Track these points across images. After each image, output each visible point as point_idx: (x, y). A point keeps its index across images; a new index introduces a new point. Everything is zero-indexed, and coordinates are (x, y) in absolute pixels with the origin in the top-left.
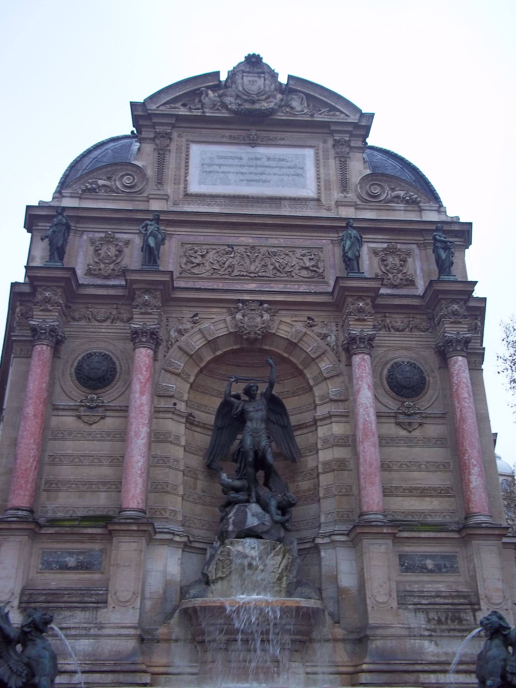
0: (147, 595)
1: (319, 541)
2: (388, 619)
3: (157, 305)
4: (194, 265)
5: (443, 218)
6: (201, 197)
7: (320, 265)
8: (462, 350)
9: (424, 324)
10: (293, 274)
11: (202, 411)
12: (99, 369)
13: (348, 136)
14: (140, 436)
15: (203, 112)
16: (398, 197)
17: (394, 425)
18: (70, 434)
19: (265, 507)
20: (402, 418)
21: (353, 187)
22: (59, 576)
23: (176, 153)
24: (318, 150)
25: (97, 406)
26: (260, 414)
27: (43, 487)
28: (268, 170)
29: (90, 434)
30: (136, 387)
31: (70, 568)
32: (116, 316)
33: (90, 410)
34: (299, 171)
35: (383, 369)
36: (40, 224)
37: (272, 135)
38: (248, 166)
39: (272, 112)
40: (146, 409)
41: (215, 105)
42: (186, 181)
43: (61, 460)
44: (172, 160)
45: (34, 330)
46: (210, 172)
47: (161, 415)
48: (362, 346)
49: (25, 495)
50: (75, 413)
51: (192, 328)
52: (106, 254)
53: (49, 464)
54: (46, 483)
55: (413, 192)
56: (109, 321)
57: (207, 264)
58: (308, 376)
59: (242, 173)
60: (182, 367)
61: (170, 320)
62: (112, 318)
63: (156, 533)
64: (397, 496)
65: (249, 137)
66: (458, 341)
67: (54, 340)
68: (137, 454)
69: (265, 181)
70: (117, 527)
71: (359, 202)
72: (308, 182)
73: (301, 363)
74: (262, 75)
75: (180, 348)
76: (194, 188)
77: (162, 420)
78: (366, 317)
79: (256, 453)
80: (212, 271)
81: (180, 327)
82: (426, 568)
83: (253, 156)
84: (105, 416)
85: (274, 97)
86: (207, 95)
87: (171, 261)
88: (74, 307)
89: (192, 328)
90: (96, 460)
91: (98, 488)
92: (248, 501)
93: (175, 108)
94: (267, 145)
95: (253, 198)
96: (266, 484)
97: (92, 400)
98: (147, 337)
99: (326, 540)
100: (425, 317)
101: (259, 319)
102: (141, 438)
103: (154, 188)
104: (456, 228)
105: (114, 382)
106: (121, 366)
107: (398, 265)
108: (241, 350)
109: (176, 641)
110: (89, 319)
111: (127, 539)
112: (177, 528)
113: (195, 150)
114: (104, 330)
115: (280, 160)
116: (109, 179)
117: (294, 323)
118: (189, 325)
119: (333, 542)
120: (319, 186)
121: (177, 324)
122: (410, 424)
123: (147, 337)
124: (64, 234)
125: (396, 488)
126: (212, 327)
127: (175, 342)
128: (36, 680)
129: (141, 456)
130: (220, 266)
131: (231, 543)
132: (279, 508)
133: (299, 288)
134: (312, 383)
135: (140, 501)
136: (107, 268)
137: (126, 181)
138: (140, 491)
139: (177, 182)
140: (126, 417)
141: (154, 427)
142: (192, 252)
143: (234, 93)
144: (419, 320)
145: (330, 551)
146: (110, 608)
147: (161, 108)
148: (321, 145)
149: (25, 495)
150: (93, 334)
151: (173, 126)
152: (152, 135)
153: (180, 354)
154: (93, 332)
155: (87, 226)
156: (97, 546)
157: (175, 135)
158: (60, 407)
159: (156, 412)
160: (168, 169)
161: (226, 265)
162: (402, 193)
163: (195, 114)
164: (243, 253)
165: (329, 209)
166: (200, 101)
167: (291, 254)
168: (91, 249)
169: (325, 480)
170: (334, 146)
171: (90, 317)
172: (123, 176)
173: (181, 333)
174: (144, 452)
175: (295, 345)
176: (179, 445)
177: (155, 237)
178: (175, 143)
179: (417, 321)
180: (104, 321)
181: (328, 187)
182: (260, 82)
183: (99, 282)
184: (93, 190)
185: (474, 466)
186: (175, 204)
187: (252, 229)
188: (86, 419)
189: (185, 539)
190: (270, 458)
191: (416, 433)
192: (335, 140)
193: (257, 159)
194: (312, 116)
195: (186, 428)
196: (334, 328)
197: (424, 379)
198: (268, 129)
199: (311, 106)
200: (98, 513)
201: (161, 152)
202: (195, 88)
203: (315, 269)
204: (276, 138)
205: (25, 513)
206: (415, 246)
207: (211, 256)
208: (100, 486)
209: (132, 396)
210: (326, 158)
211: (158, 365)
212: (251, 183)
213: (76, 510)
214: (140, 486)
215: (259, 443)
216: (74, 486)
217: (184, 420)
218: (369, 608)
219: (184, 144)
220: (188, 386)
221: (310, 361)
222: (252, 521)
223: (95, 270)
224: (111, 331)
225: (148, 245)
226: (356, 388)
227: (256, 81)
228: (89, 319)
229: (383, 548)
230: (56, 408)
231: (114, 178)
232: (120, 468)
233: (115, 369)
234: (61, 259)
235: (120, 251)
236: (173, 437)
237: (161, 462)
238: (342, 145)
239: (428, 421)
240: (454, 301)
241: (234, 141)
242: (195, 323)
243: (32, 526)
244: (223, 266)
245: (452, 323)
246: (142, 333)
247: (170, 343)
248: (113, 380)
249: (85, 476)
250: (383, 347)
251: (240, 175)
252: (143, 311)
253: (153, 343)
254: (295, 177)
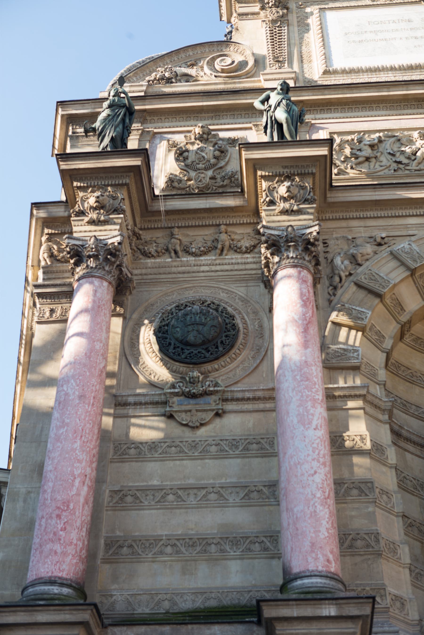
3: (309, 197)
4: (360, 159)
11: (413, 415)
12: (204, 325)
14: (310, 423)
23: (299, 26)
25: (206, 394)
27: (101, 554)
29: (194, 446)
32: (227, 244)
33: (192, 401)
43: (137, 498)
49: (64, 554)
50: (161, 410)
51: (375, 253)
52: (198, 156)
53: (114, 509)
54: (108, 545)
57: (382, 158)
59: (416, 38)
60: (369, 316)
61: (331, 243)
62: (220, 246)
68: (310, 459)
75: (359, 286)
84: (224, 412)
89: (375, 253)
90: (213, 496)
91: (222, 551)
98: (298, 249)
102: (314, 426)
105: (235, 350)
106: (245, 323)
110: (176, 252)
118: (369, 249)
121: (346, 247)
123: (298, 249)
124: (123, 120)
127: (346, 276)
129: (318, 461)
130: (409, 158)
135: (331, 557)
136: (203, 175)
138: (326, 534)
149: (64, 554)
150: (186, 275)
153: (362, 294)
154: (184, 273)
158: (131, 400)
171: (178, 248)
174: (324, 456)
176: (384, 463)
178: (295, 15)
180: (204, 253)
188: (184, 418)
205: (65, 591)
208: (228, 548)
213: (177, 599)
214: (324, 523)
216: (169, 550)
217: (386, 417)
224: (218, 268)
228: (176, 252)
232: (266, 508)
237: (355, 492)
242: (380, 245)
244: (413, 158)
246: (287, 241)
247: (337, 279)
248: (232, 346)
249: (192, 529)
253: (310, 261)
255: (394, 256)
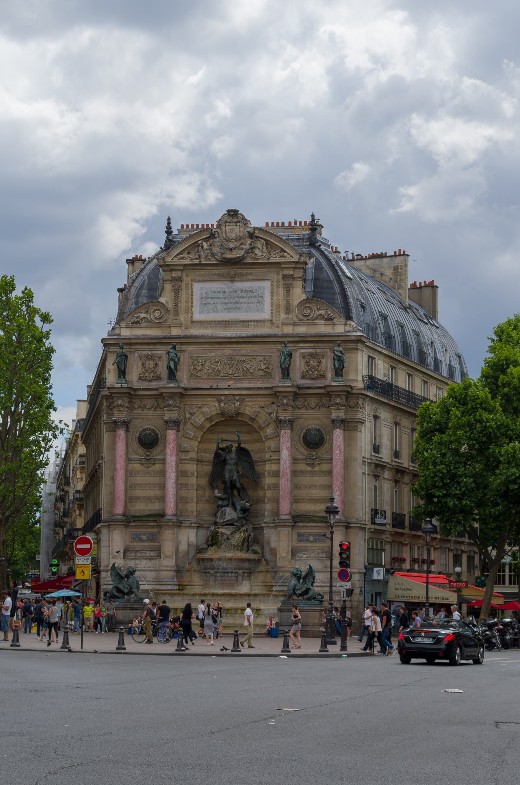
0: (180, 551)
1: (263, 525)
2: (286, 564)
5: (348, 328)
6: (201, 323)
7: (270, 367)
8: (340, 425)
9: (328, 403)
10: (254, 374)
13: (292, 270)
15: (200, 261)
16: (321, 315)
17: (304, 465)
18: (138, 473)
19: (235, 509)
20: (309, 461)
21: (294, 308)
22: (140, 544)
24: (272, 282)
25: (151, 459)
26: (234, 461)
27: (128, 501)
28: (242, 300)
29: (148, 473)
30: (168, 452)
31: (144, 541)
34: (260, 299)
35: (301, 432)
36: (110, 348)
37: (244, 271)
38: (229, 298)
39: (243, 258)
40: (174, 464)
41: (207, 256)
42: (192, 311)
44: (183, 295)
45: (115, 422)
46: (206, 304)
47: (183, 462)
48: (285, 425)
50: (140, 462)
51: (198, 411)
54: (129, 499)
55: (331, 311)
56: (153, 409)
57: (205, 370)
58: (262, 435)
61: (186, 406)
63: (182, 523)
64: (303, 503)
65: (229, 275)
66: (337, 421)
67: (126, 426)
69: (239, 309)
70: (162, 524)
71: (296, 319)
72: (265, 307)
73: (259, 427)
74: (238, 224)
75: (192, 424)
76: (197, 316)
77: (184, 465)
78: (288, 408)
79: (231, 482)
80: (208, 374)
81: (191, 411)
82: (310, 540)
83: (232, 290)
85: (245, 245)
86: (202, 247)
87: (185, 368)
88: (134, 400)
89: (198, 411)
92: (227, 506)
93: (182, 258)
94: (241, 280)
95: (231, 321)
96: (239, 495)
97: (147, 455)
99: (266, 525)
100: (328, 399)
101: (233, 406)
103: (173, 318)
104: (353, 338)
107: (316, 365)
108: (226, 420)
109: (195, 571)
111: (168, 528)
112: (193, 519)
113: (197, 286)
114: (151, 414)
115: (249, 291)
116: (147, 312)
117: (254, 406)
118: (196, 410)
119: (268, 526)
120: (272, 310)
122: (313, 464)
125: (303, 499)
126: (208, 411)
128: (133, 590)
131: (218, 528)
132: (241, 510)
133: (257, 383)
134: (264, 439)
137: (157, 314)
139: (186, 313)
140: (165, 463)
141: (180, 468)
142: (196, 362)
143: (219, 244)
144: (325, 400)
145: (268, 530)
146: (162, 559)
147: (175, 258)
148: (275, 277)
151: (183, 270)
152: (170, 278)
153: (192, 427)
155: (136, 347)
156: (155, 530)
157: (184, 275)
159: (180, 461)
160: (181, 302)
161: (216, 370)
162: (322, 312)
163: (195, 263)
164: (226, 361)
165: (278, 327)
166: (198, 252)
167: (253, 360)
168: (140, 363)
169: (269, 494)
170: (283, 278)
172: (154, 311)
173: (191, 414)
175: (254, 419)
177: (174, 360)
179: (324, 401)
181: (278, 311)
182: (237, 229)
183: (146, 385)
184: (138, 322)
185: (337, 490)
186: (186, 328)
187: (231, 344)
189: (197, 525)
190: (238, 485)
191: (317, 468)
192: (283, 275)
193: (235, 292)
194: (268, 259)
195: (197, 465)
196: (276, 408)
197: (323, 438)
198: (242, 267)
199: (269, 247)
200: (155, 513)
201: (176, 292)
202: (195, 241)
203: (267, 370)
204: (247, 273)
206: (328, 350)
207: (208, 363)
209: (167, 456)
210: (278, 287)
211: (180, 434)
212: (231, 310)
215: (233, 476)
218: (278, 559)
219: (190, 282)
220: (197, 443)
221: (261, 428)
222: (228, 518)
223: (143, 377)
225: (170, 367)
226: (281, 448)
227: (234, 229)
229: (286, 532)
230: (130, 460)
231: (149, 312)
233: (158, 438)
234: (124, 377)
235: (156, 365)
236: (189, 473)
238: (288, 278)
239: (324, 461)
240: (338, 396)
241: (221, 278)
243: (125, 523)
245: (336, 409)
248: (157, 444)
250: (303, 418)
251: (224, 305)
252: (169, 409)
254: (258, 304)
255: (202, 413)
